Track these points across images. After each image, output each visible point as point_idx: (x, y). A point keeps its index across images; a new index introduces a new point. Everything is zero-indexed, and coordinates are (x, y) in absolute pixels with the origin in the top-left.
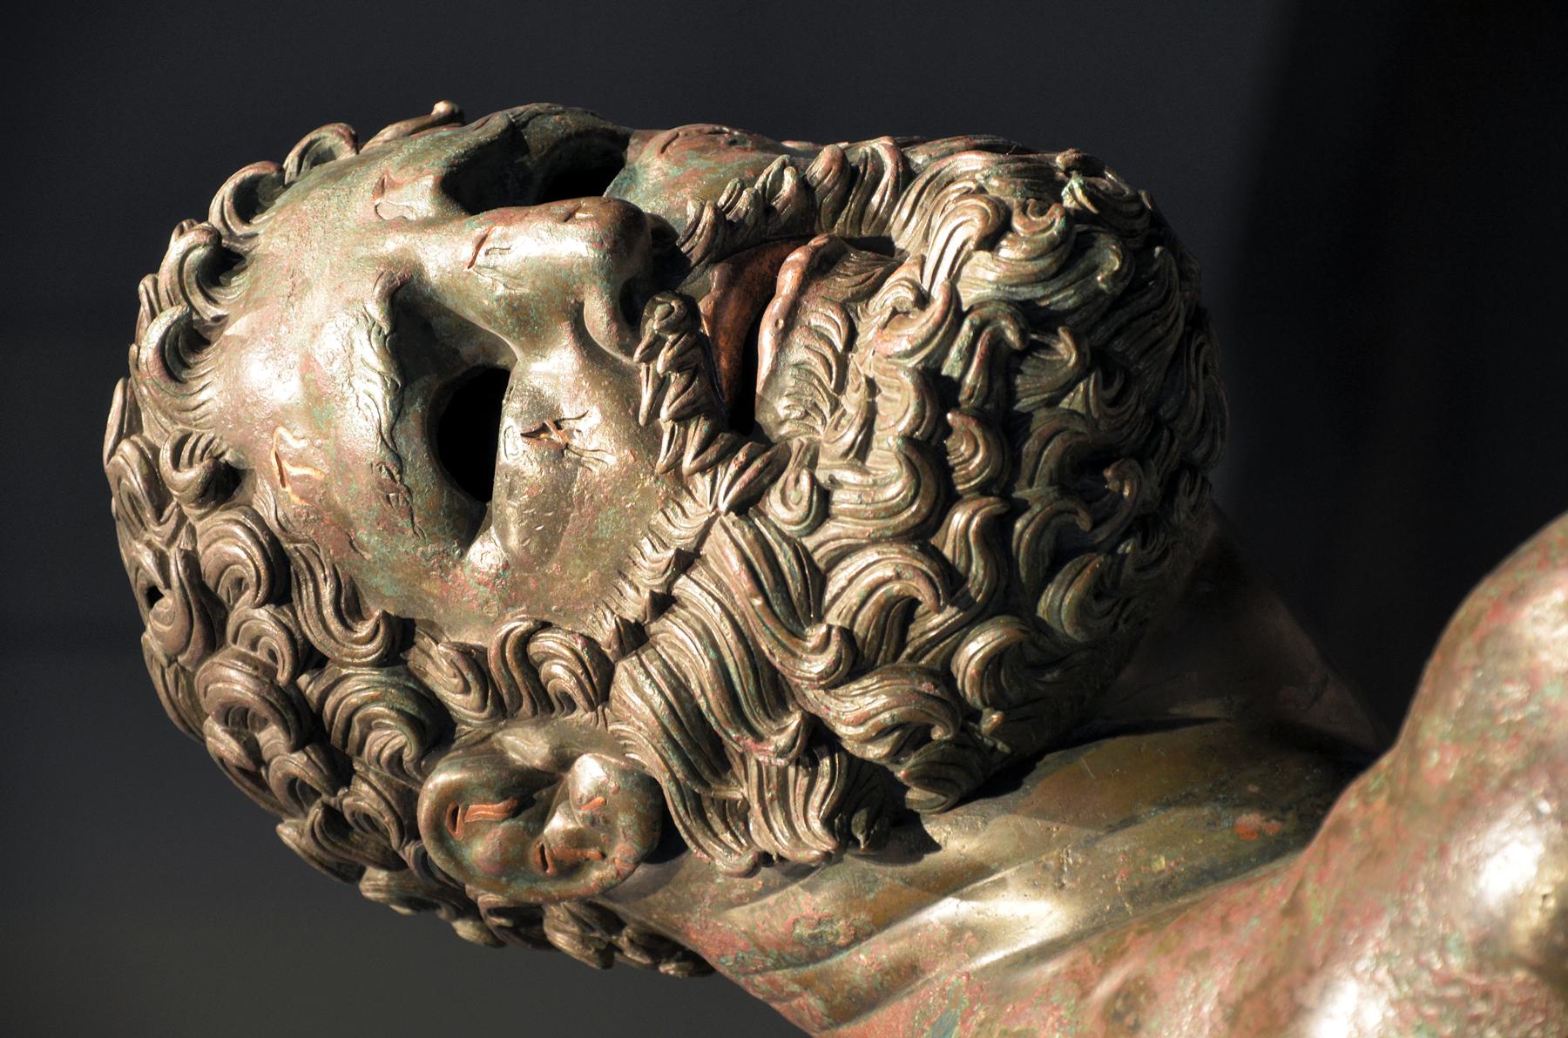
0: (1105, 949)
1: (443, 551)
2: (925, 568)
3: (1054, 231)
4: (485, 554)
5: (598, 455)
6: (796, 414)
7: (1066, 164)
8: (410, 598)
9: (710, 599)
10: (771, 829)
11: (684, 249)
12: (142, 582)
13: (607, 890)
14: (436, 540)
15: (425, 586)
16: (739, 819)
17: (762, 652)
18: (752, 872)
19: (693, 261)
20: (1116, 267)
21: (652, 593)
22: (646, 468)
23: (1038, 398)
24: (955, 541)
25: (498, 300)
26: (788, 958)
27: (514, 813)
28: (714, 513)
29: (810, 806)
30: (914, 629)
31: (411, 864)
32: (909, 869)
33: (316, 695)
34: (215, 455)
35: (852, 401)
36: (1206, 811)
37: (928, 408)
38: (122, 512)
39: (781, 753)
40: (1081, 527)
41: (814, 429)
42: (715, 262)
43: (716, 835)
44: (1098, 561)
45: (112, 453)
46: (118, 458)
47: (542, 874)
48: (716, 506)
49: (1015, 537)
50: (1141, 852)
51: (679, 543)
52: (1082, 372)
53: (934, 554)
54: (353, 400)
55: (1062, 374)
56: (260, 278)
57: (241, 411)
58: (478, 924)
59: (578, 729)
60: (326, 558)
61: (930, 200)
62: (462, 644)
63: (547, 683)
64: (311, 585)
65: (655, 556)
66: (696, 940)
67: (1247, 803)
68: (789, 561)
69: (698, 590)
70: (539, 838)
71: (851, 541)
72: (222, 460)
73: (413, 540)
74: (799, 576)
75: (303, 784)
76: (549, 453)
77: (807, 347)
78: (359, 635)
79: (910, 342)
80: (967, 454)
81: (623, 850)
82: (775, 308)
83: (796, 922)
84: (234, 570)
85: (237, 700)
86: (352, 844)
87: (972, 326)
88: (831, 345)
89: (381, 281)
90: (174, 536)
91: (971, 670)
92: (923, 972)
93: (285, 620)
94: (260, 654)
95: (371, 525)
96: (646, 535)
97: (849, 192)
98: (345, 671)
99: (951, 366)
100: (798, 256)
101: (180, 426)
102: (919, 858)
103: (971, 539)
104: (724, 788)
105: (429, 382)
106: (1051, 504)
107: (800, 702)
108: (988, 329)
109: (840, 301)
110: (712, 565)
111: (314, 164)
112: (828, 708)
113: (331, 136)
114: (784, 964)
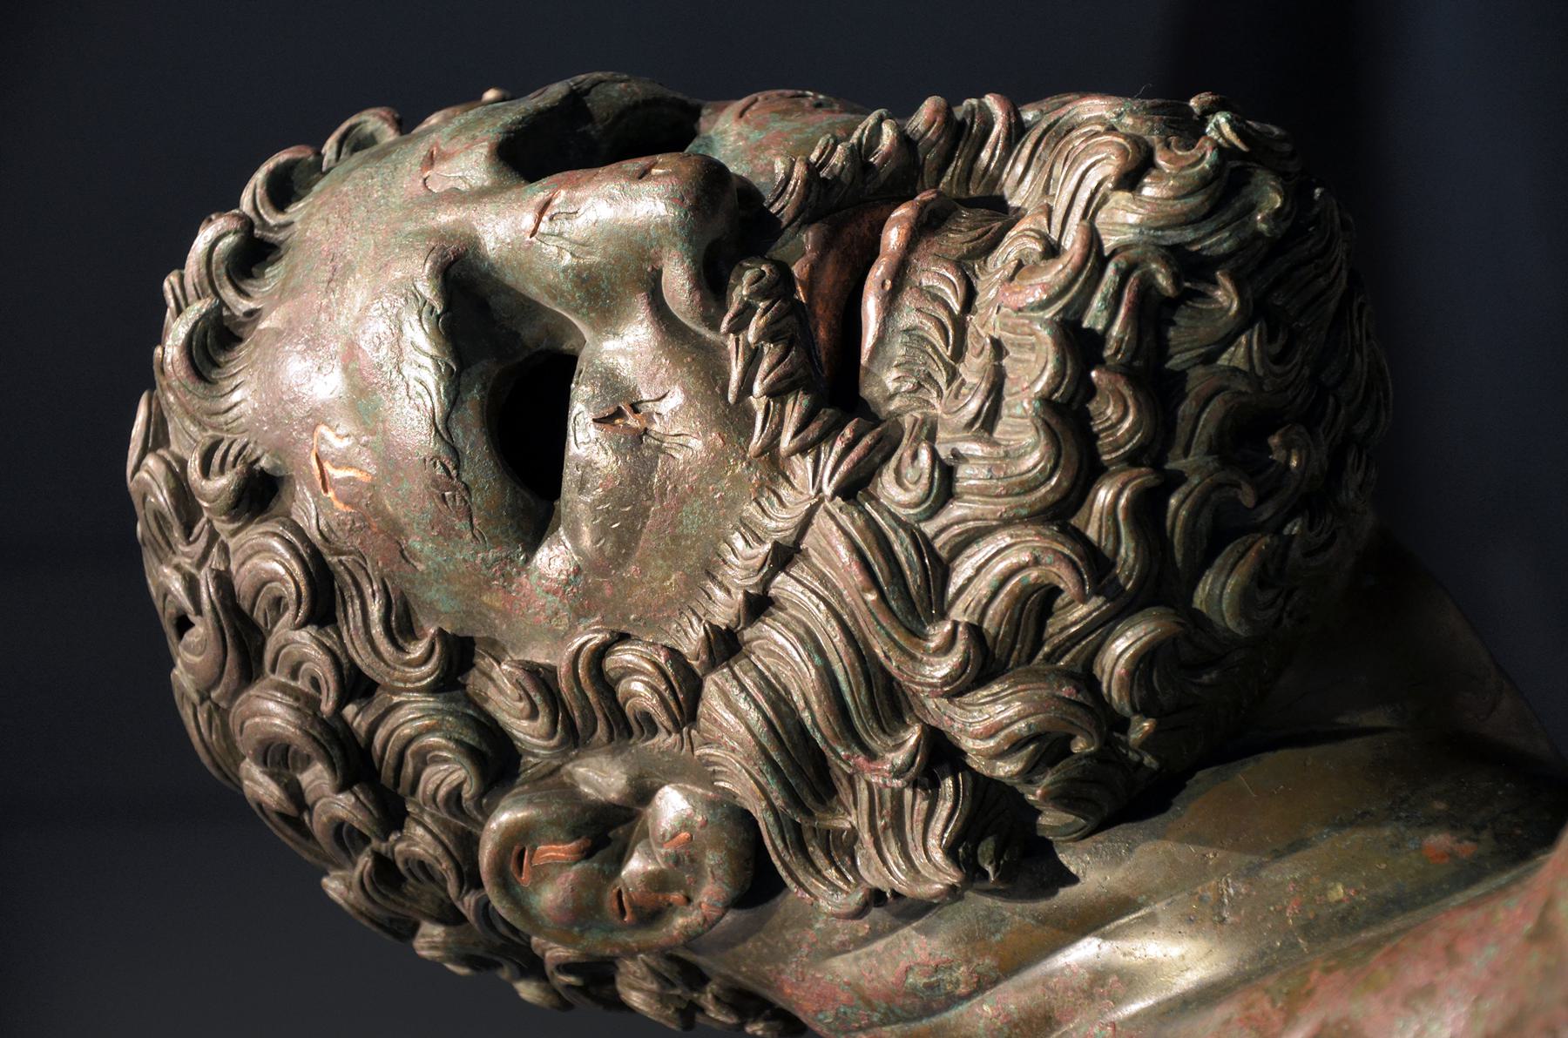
0: (1285, 990)
1: (506, 557)
2: (1067, 552)
3: (1205, 165)
4: (553, 559)
5: (681, 440)
6: (908, 386)
7: (1202, 107)
8: (469, 614)
9: (814, 597)
10: (884, 862)
11: (773, 210)
12: (171, 610)
13: (692, 940)
14: (498, 544)
15: (485, 598)
16: (844, 853)
17: (875, 656)
18: (860, 913)
19: (785, 222)
20: (1278, 205)
21: (746, 594)
22: (737, 453)
23: (1194, 353)
24: (1101, 519)
25: (565, 270)
26: (898, 1011)
27: (587, 854)
28: (816, 500)
29: (930, 835)
30: (1052, 624)
31: (471, 917)
32: (1042, 905)
33: (364, 726)
34: (249, 461)
35: (973, 369)
36: (1387, 832)
37: (1069, 364)
38: (148, 535)
39: (898, 773)
40: (1245, 503)
41: (928, 402)
42: (808, 222)
43: (819, 872)
44: (1263, 542)
45: (137, 469)
46: (143, 475)
47: (619, 922)
48: (820, 490)
49: (1170, 514)
50: (1315, 880)
51: (775, 537)
52: (1245, 322)
53: (1077, 536)
54: (402, 389)
55: (1222, 326)
56: (296, 265)
57: (277, 411)
58: (544, 984)
59: (660, 756)
60: (374, 571)
62: (528, 662)
63: (625, 703)
64: (357, 602)
65: (749, 552)
66: (791, 995)
67: (1433, 822)
68: (907, 549)
69: (800, 588)
70: (616, 881)
71: (979, 523)
72: (257, 467)
73: (473, 545)
74: (918, 567)
75: (352, 828)
76: (626, 439)
77: (918, 310)
78: (412, 656)
79: (1045, 291)
80: (1114, 417)
81: (710, 892)
82: (878, 272)
83: (908, 970)
84: (272, 588)
85: (276, 736)
86: (404, 896)
87: (1118, 270)
88: (946, 306)
89: (433, 255)
90: (205, 555)
91: (1120, 669)
92: (1059, 1023)
93: (328, 643)
94: (302, 684)
95: (424, 530)
96: (738, 529)
97: (954, 147)
98: (396, 699)
99: (1094, 317)
100: (903, 211)
101: (210, 432)
102: (1054, 893)
103: (1121, 516)
104: (829, 816)
105: (486, 366)
106: (1210, 475)
107: (918, 714)
108: (1136, 274)
109: (955, 258)
110: (816, 559)
111: (354, 150)
112: (952, 719)
113: (373, 121)
114: (893, 1019)
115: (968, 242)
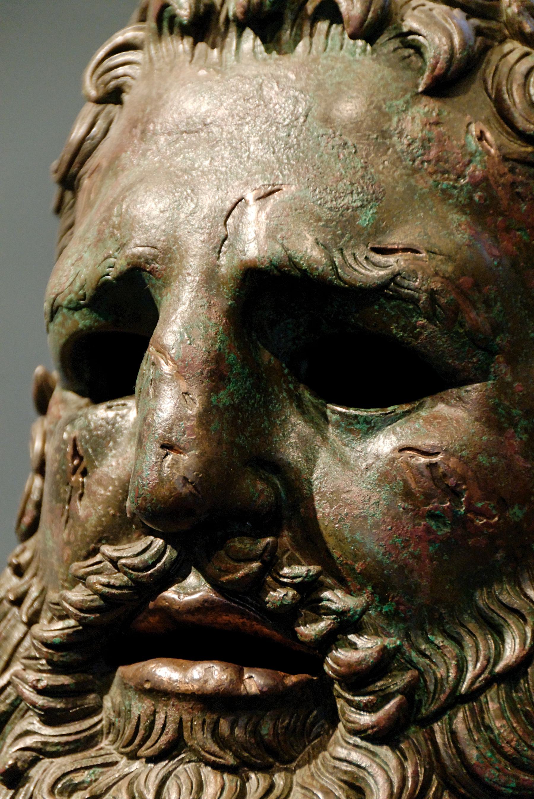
61: (340, 775)
77: (139, 718)
89: (147, 250)
115: (198, 744)
